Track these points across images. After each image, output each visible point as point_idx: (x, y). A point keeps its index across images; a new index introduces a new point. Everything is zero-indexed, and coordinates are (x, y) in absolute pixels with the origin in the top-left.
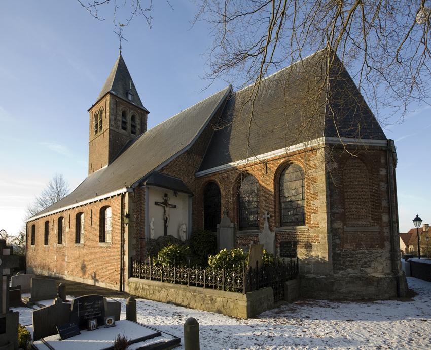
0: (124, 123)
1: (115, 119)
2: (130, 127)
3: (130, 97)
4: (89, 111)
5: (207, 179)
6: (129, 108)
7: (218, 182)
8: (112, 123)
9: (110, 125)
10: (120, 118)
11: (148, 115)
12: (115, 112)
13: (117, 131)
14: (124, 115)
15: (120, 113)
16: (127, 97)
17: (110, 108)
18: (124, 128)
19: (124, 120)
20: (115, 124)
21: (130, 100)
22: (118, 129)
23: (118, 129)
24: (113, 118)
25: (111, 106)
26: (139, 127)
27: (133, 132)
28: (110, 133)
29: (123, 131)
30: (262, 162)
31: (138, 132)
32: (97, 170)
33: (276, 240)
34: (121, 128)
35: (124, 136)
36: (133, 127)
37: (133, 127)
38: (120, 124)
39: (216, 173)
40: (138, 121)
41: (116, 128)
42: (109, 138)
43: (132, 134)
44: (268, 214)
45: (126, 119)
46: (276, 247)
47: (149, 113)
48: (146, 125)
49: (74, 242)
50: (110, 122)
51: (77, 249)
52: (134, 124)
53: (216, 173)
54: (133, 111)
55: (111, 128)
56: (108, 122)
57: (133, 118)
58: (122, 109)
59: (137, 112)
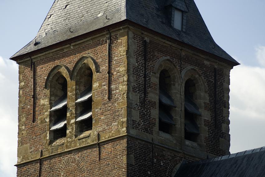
0: (165, 109)
2: (183, 120)
3: (177, 21)
8: (136, 115)
9: (131, 124)
10: (154, 96)
11: (235, 74)
13: (147, 137)
15: (155, 80)
16: (169, 21)
17: (128, 70)
18: (165, 127)
19: (165, 101)
20: (143, 116)
21: (178, 33)
22: (151, 133)
23: (151, 133)
24: (136, 98)
25: (133, 61)
26: (206, 115)
27: (190, 136)
28: (129, 149)
29: (164, 136)
31: (204, 133)
34: (156, 128)
36: (191, 117)
37: (191, 117)
38: (155, 113)
41: (146, 130)
43: (188, 142)
45: (169, 97)
48: (226, 105)
50: (129, 114)
52: (191, 109)
54: (190, 67)
55: (133, 132)
56: (124, 112)
57: (190, 86)
58: (161, 66)
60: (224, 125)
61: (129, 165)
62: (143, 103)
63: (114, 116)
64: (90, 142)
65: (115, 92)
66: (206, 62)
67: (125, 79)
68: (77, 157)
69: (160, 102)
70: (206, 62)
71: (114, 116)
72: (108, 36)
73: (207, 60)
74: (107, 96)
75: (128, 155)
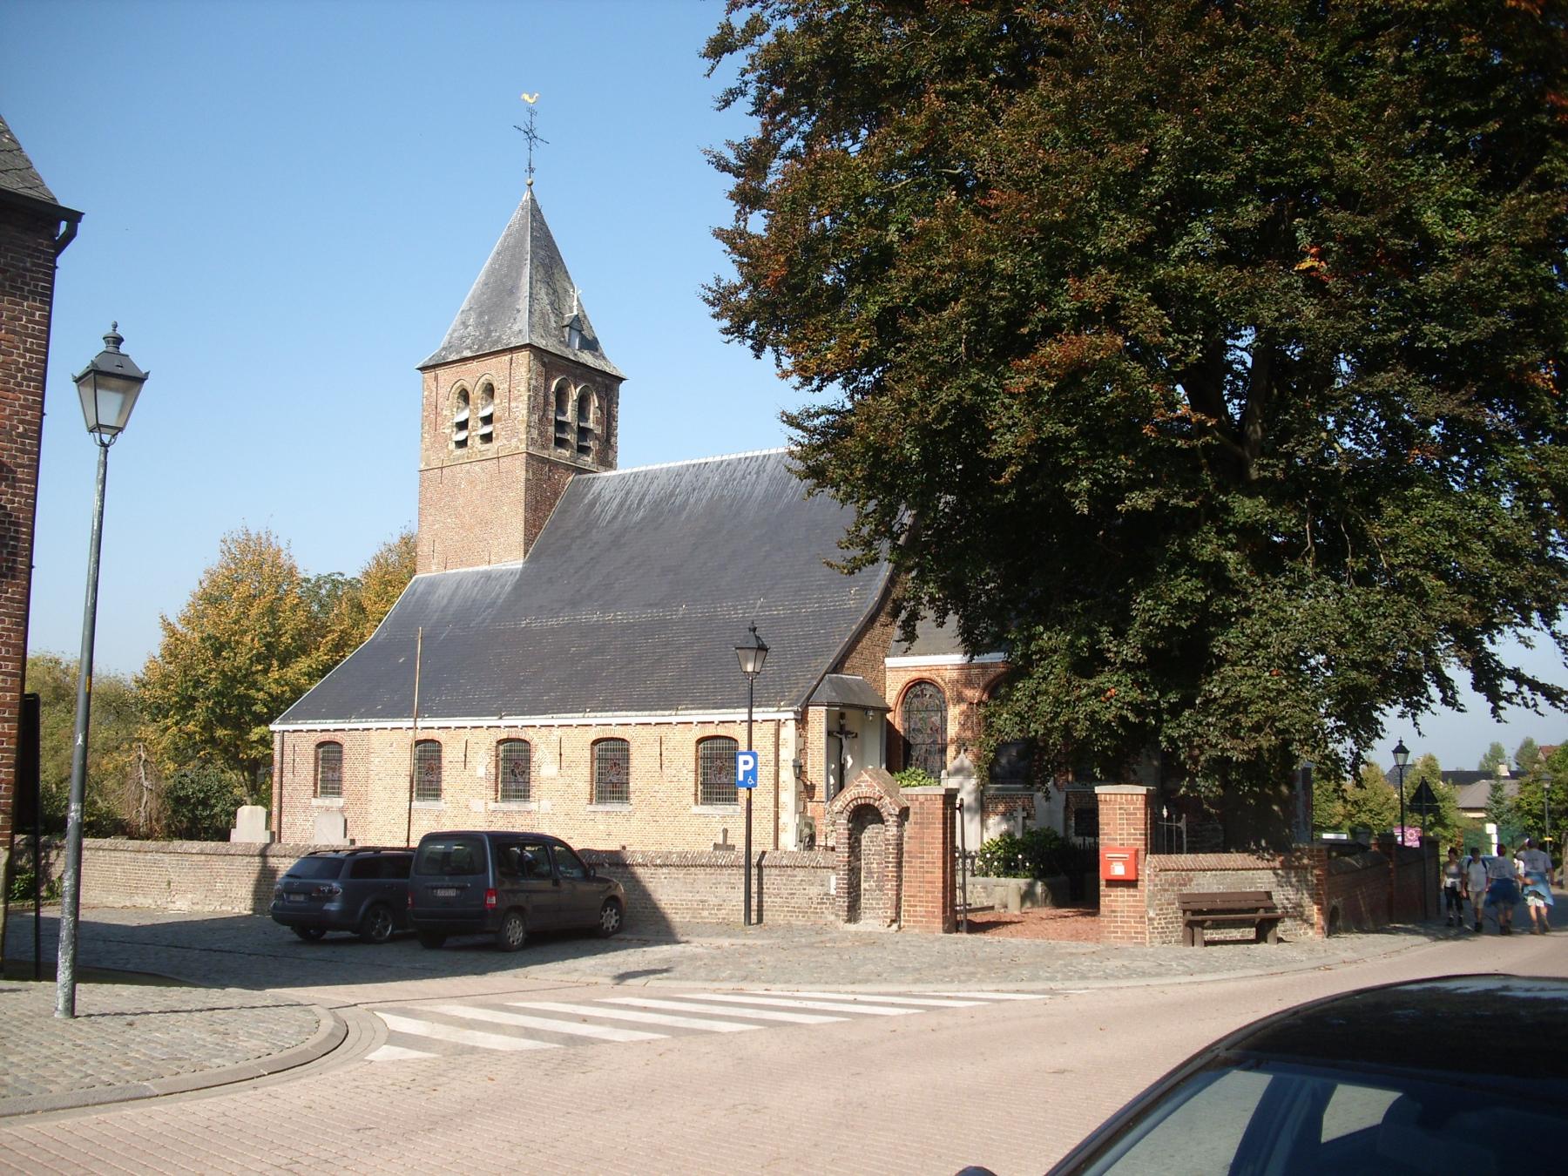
4: (423, 369)
5: (916, 675)
6: (575, 377)
8: (535, 433)
14: (561, 394)
32: (462, 564)
33: (1067, 807)
42: (527, 480)
46: (1066, 819)
47: (621, 380)
49: (587, 801)
51: (599, 816)
62: (543, 420)
63: (514, 433)
64: (490, 455)
68: (477, 468)
70: (598, 379)
71: (514, 433)
75: (527, 471)
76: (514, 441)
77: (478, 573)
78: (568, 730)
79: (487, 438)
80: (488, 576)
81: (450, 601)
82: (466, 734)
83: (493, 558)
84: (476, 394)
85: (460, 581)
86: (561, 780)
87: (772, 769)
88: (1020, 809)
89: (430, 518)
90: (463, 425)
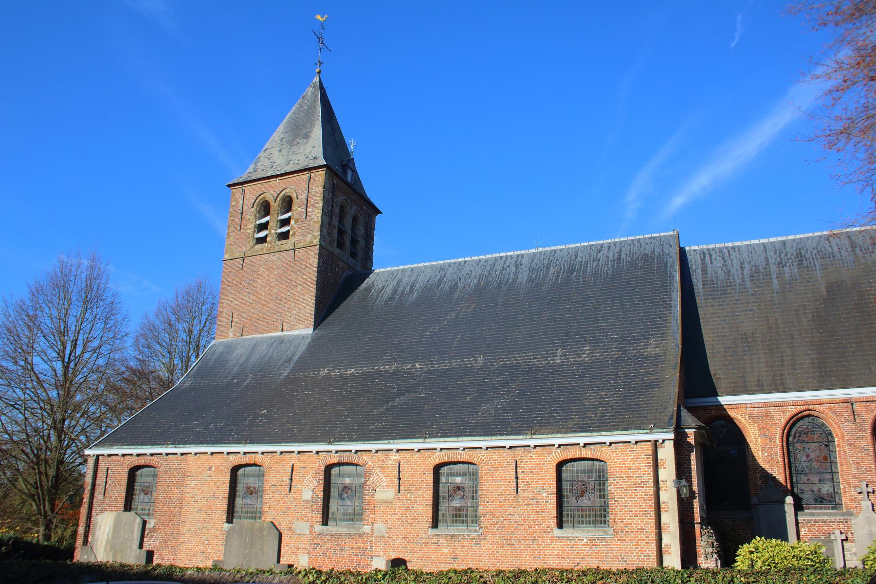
0: (341, 232)
1: (330, 224)
7: (743, 420)
8: (325, 231)
9: (322, 238)
10: (335, 222)
11: (378, 218)
12: (330, 208)
13: (329, 248)
15: (337, 211)
20: (329, 234)
25: (326, 194)
26: (362, 243)
30: (845, 401)
35: (341, 264)
37: (354, 242)
39: (740, 406)
40: (361, 231)
44: (867, 486)
50: (321, 230)
53: (740, 406)
55: (323, 243)
57: (355, 219)
59: (362, 208)
60: (370, 252)
61: (319, 266)
63: (309, 231)
64: (287, 247)
65: (311, 214)
66: (364, 207)
67: (321, 205)
69: (339, 227)
70: (364, 207)
71: (309, 231)
72: (309, 175)
73: (366, 206)
74: (304, 217)
76: (309, 237)
77: (271, 338)
78: (408, 455)
79: (285, 236)
80: (281, 340)
81: (248, 358)
82: (294, 459)
83: (285, 326)
84: (275, 206)
85: (256, 344)
86: (399, 504)
87: (651, 491)
88: (837, 532)
89: (230, 296)
90: (263, 227)
